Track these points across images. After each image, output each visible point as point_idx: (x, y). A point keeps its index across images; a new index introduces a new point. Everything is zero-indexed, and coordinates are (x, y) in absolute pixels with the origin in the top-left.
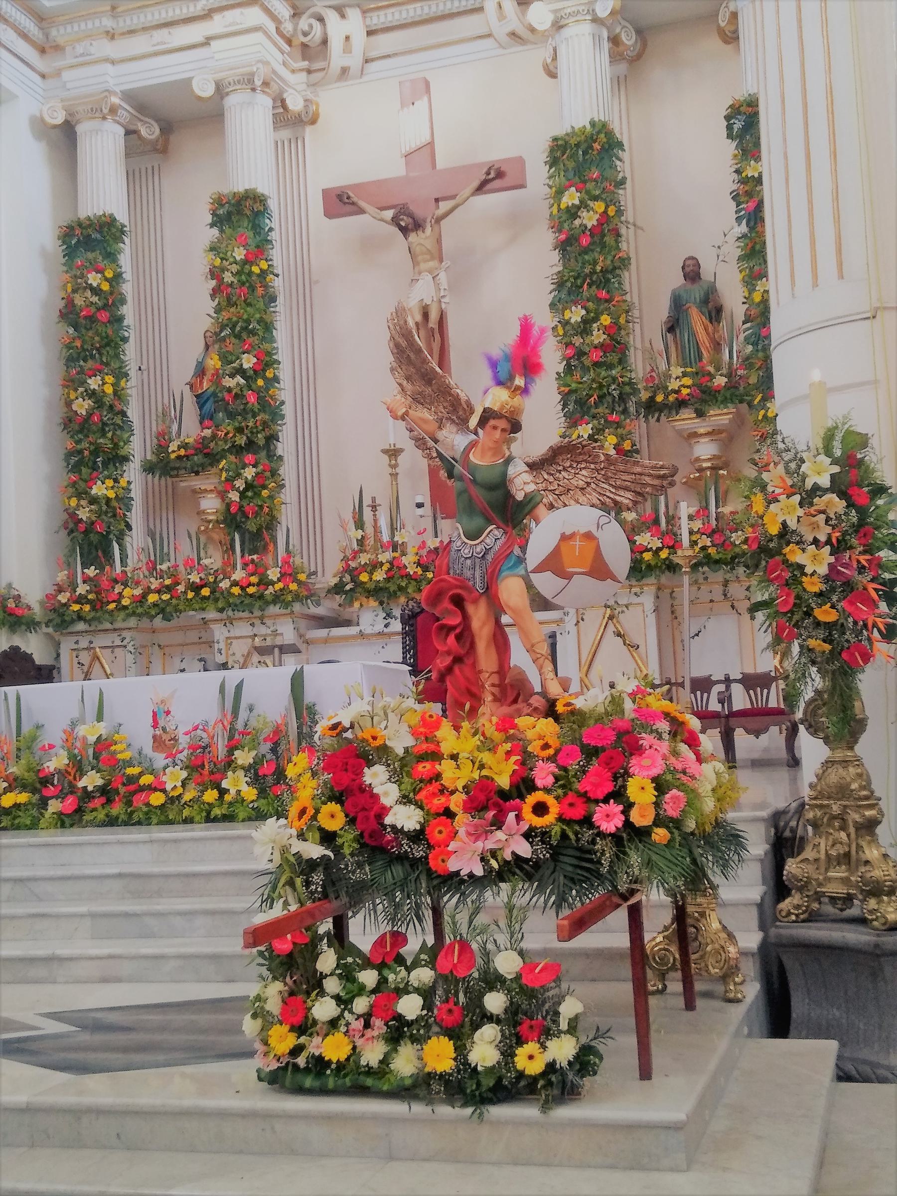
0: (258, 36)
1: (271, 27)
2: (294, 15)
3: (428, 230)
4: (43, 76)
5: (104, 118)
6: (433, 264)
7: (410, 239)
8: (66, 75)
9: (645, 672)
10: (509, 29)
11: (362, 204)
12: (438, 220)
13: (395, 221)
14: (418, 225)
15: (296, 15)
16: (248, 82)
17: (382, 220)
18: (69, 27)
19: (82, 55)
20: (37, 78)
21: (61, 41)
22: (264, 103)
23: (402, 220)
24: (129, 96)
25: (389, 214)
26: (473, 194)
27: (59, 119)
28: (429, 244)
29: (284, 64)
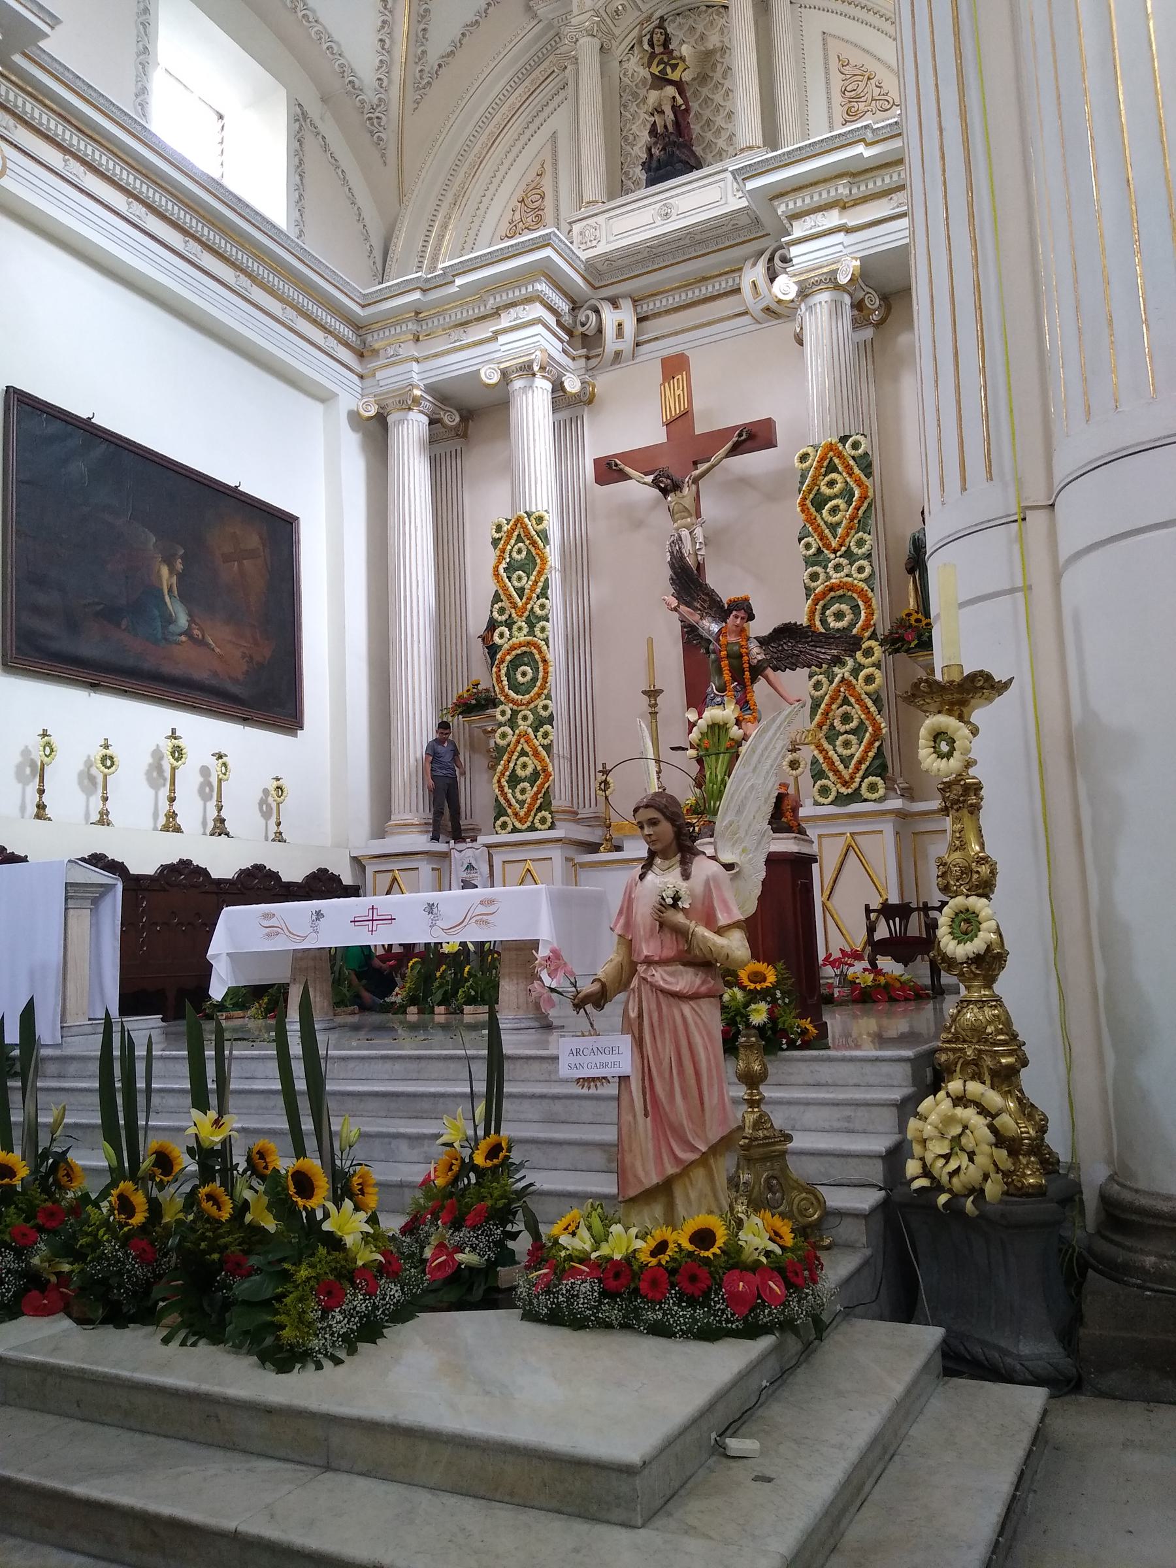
0: (539, 328)
1: (551, 320)
2: (573, 309)
3: (686, 490)
4: (361, 377)
5: (410, 409)
6: (689, 520)
7: (669, 499)
8: (379, 375)
9: (885, 897)
10: (764, 305)
11: (628, 470)
12: (696, 481)
13: (656, 483)
14: (676, 487)
15: (575, 307)
16: (527, 369)
17: (644, 483)
18: (381, 333)
19: (392, 356)
20: (355, 379)
21: (376, 346)
22: (543, 385)
23: (662, 482)
24: (429, 389)
25: (650, 479)
26: (728, 455)
27: (373, 412)
28: (688, 502)
29: (564, 351)
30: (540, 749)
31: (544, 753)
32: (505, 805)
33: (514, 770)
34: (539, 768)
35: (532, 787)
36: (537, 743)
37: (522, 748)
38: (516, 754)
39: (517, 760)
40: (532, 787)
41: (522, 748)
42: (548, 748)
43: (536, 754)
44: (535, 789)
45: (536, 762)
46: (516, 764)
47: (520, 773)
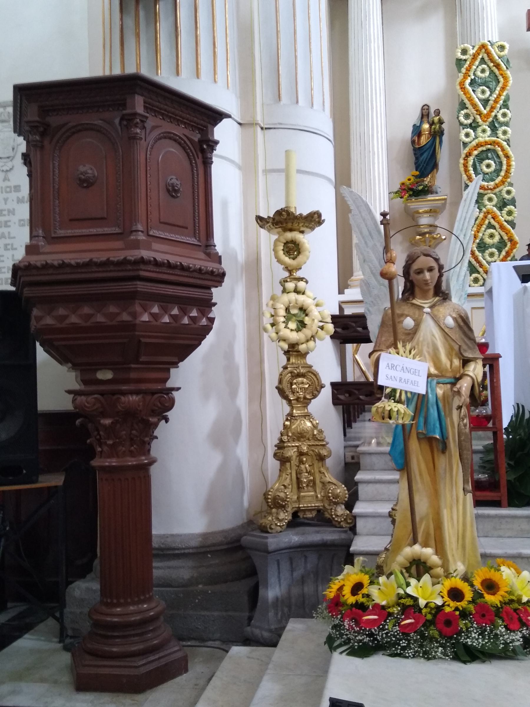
30: (505, 224)
31: (509, 227)
32: (477, 265)
33: (482, 239)
34: (505, 238)
35: (500, 251)
36: (503, 219)
37: (489, 223)
38: (485, 226)
39: (485, 231)
40: (500, 251)
41: (489, 223)
42: (512, 224)
43: (502, 227)
44: (503, 253)
45: (503, 234)
46: (483, 234)
47: (488, 241)
